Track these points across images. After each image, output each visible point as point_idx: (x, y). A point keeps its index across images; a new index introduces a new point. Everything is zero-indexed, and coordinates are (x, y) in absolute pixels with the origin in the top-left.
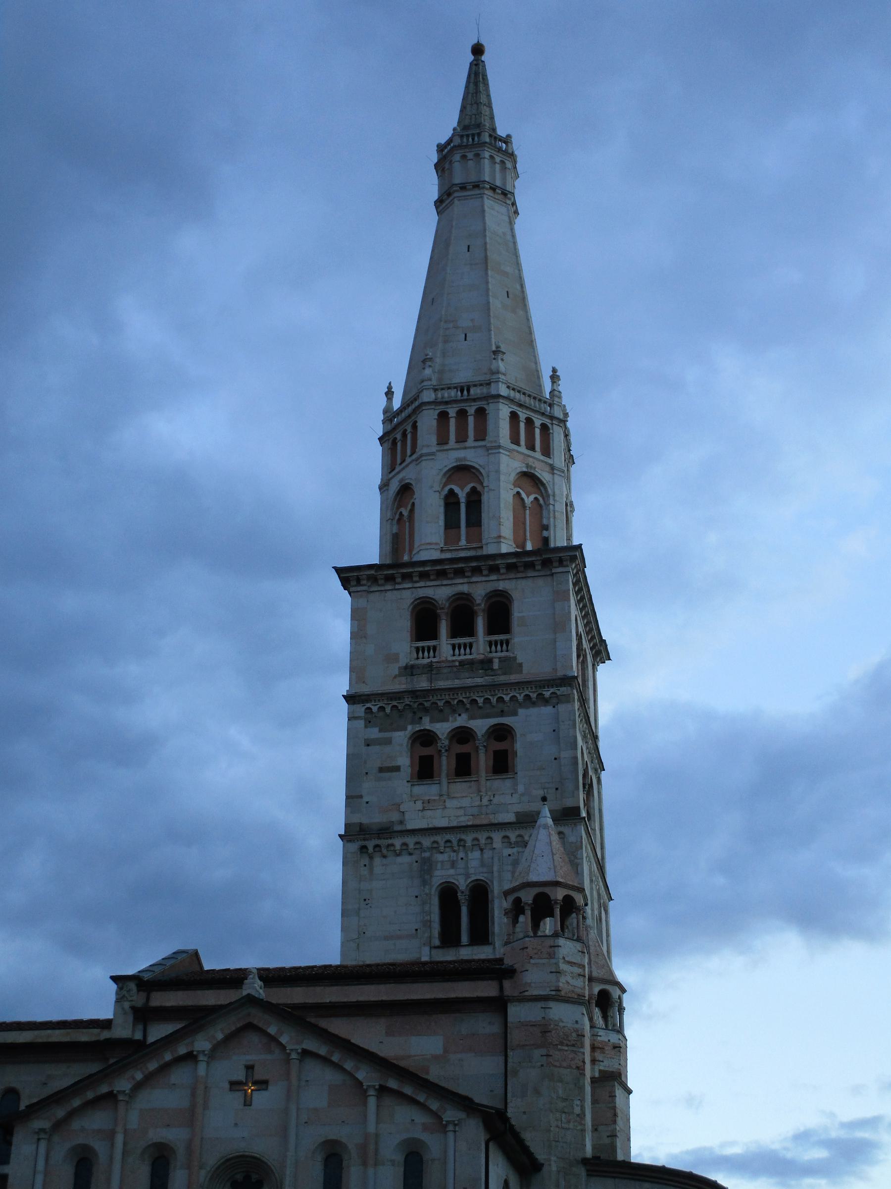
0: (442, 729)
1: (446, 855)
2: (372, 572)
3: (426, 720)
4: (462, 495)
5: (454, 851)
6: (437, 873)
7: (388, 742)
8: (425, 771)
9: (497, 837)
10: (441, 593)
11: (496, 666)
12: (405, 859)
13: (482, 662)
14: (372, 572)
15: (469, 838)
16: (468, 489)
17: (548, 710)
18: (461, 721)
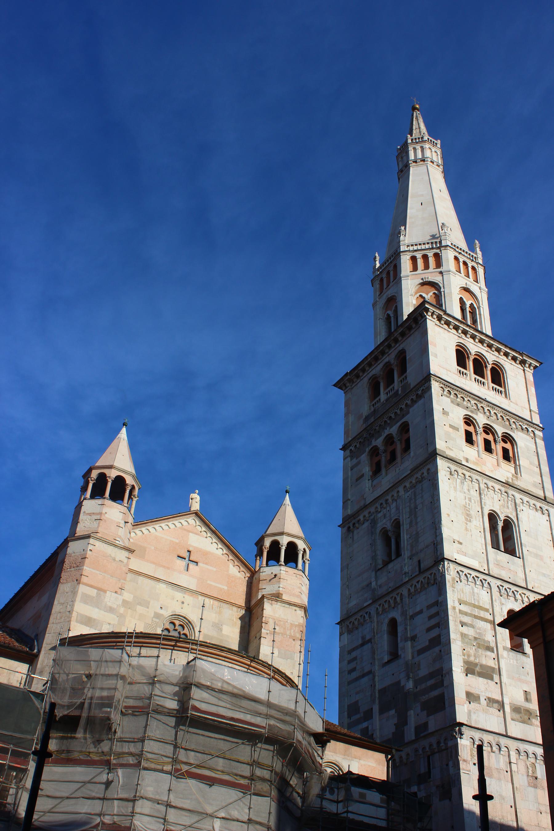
0: (379, 442)
1: (382, 512)
2: (349, 377)
3: (373, 441)
4: (390, 313)
5: (385, 508)
6: (379, 525)
7: (358, 463)
8: (377, 470)
9: (401, 489)
10: (377, 369)
11: (400, 392)
12: (366, 524)
13: (394, 393)
14: (349, 377)
15: (389, 497)
16: (393, 308)
17: (423, 399)
18: (387, 432)
